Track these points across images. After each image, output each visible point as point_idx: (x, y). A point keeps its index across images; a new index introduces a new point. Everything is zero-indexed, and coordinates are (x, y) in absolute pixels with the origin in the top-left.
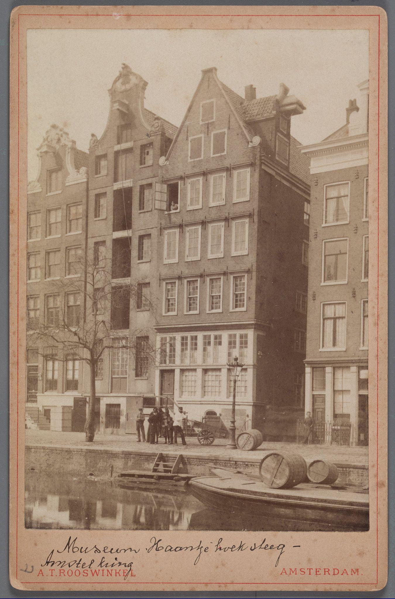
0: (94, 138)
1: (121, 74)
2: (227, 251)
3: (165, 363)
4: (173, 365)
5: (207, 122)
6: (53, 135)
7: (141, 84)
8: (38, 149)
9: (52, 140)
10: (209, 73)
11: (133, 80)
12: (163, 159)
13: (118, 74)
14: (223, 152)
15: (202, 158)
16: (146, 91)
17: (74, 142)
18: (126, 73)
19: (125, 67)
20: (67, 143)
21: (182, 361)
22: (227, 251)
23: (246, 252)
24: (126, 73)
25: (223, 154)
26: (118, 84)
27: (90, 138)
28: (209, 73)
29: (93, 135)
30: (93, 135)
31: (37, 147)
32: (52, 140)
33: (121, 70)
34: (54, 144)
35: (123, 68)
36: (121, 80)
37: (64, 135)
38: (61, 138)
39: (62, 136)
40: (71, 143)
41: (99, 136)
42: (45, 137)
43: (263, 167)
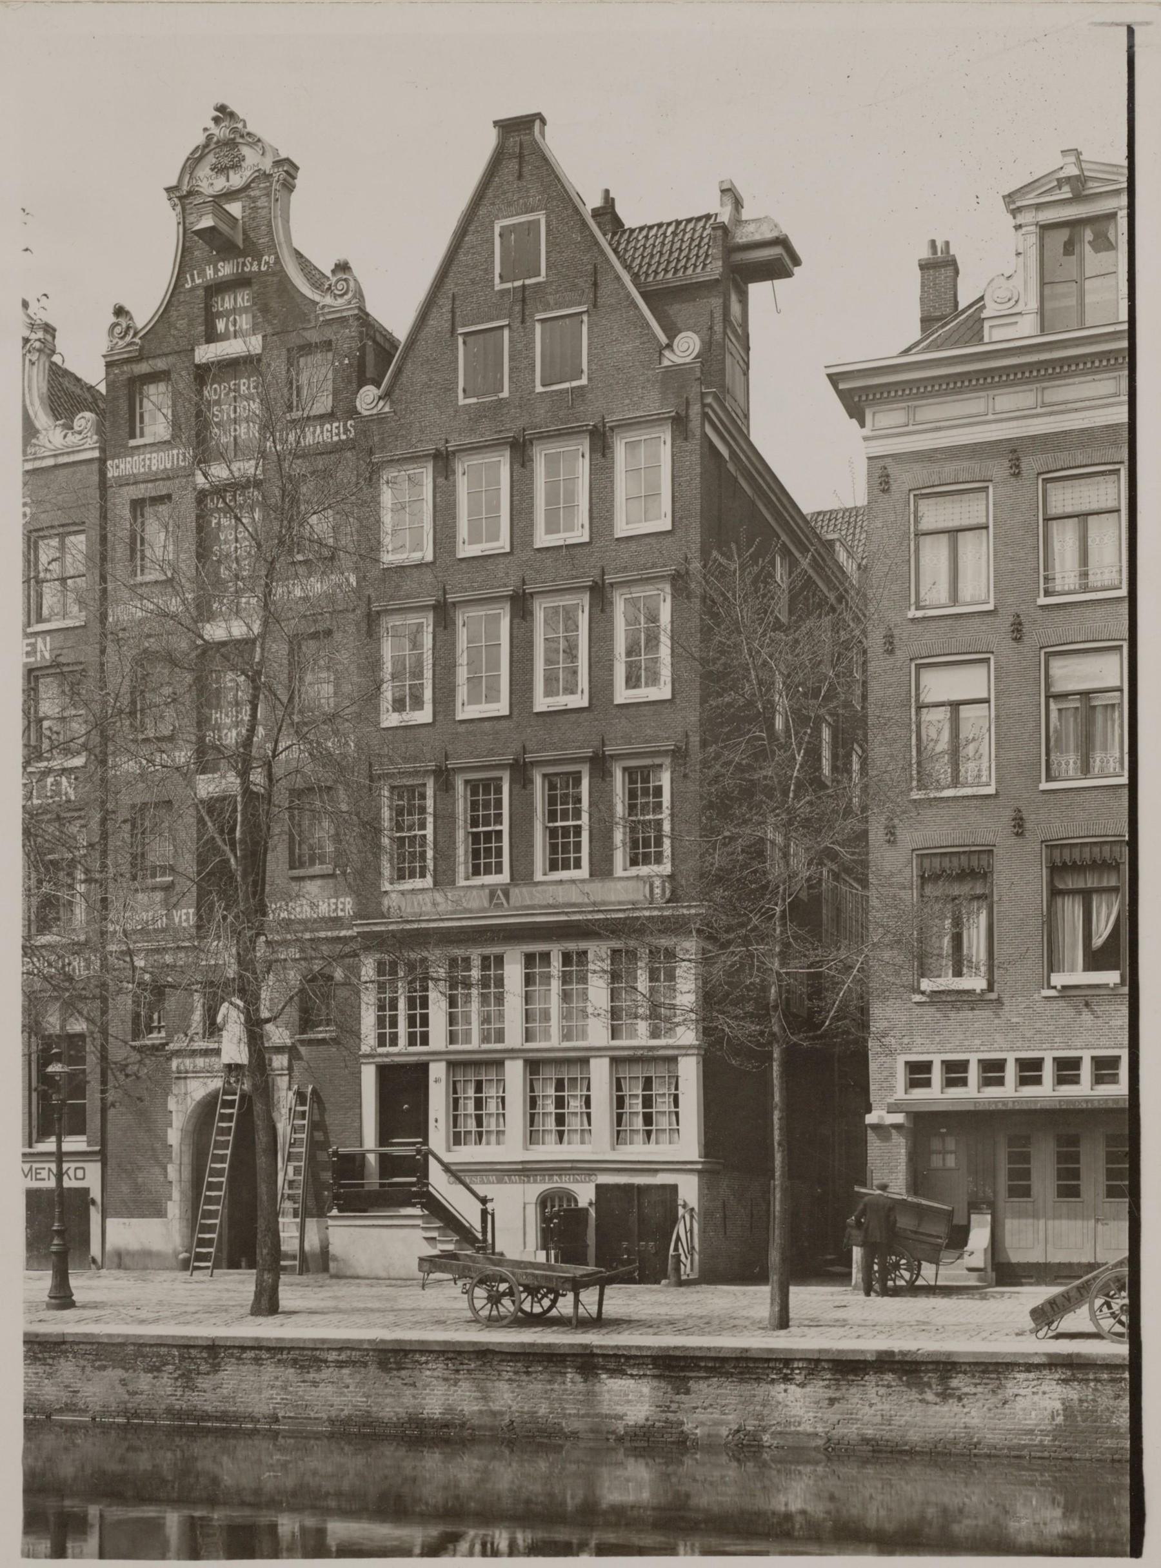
1: (209, 138)
2: (601, 686)
5: (518, 283)
7: (279, 174)
10: (519, 138)
12: (369, 393)
13: (200, 139)
14: (578, 375)
15: (505, 394)
16: (294, 196)
18: (227, 139)
19: (223, 113)
22: (601, 686)
23: (663, 691)
24: (227, 139)
25: (575, 384)
27: (113, 319)
29: (120, 311)
30: (120, 311)
33: (211, 124)
35: (216, 120)
36: (211, 159)
41: (143, 315)
43: (709, 430)
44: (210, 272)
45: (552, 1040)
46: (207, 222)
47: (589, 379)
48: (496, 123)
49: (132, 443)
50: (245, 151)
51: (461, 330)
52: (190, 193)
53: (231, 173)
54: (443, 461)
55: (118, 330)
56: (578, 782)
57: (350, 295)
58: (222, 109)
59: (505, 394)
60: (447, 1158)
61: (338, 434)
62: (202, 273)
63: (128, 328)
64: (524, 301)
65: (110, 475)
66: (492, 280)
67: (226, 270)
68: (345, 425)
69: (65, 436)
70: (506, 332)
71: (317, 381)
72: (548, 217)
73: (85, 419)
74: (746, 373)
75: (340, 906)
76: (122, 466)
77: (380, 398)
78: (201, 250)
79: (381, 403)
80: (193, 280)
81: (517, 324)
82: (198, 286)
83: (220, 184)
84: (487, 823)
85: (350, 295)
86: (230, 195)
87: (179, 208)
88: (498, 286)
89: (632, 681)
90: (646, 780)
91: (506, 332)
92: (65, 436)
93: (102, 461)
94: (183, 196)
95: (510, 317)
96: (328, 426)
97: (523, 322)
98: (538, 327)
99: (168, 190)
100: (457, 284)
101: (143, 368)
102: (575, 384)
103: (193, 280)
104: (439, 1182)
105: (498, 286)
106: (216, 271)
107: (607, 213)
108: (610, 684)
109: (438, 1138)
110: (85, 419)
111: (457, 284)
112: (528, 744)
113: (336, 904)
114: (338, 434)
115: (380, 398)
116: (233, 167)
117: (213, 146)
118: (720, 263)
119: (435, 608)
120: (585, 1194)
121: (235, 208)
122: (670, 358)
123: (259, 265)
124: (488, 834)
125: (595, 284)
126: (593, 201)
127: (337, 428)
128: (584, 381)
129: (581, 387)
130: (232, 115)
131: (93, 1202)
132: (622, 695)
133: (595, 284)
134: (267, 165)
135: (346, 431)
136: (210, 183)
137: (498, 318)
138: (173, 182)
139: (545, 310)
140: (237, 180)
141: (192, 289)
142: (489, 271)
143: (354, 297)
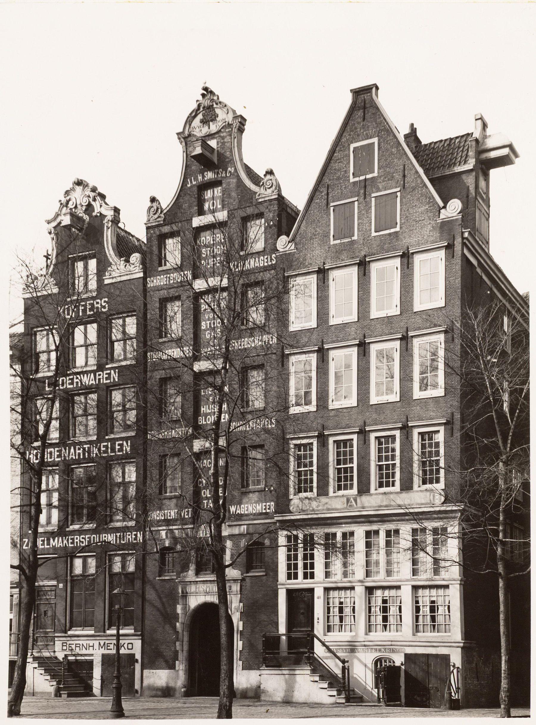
0: (155, 205)
1: (199, 106)
3: (296, 577)
4: (312, 580)
5: (362, 178)
6: (79, 197)
7: (236, 124)
8: (49, 222)
9: (76, 207)
11: (222, 115)
12: (283, 239)
13: (195, 106)
15: (355, 238)
17: (117, 210)
19: (207, 92)
20: (104, 212)
21: (327, 575)
25: (392, 230)
26: (197, 122)
27: (149, 204)
28: (364, 102)
31: (51, 216)
32: (76, 207)
33: (200, 98)
34: (80, 212)
35: (203, 95)
36: (200, 117)
37: (98, 198)
38: (93, 203)
39: (94, 200)
40: (112, 213)
41: (166, 200)
42: (64, 200)
43: (466, 251)
44: (200, 178)
45: (380, 578)
46: (198, 150)
47: (401, 228)
48: (351, 91)
49: (160, 269)
50: (218, 111)
51: (332, 204)
52: (190, 135)
53: (211, 123)
54: (322, 273)
55: (152, 210)
56: (394, 441)
57: (274, 187)
58: (206, 89)
59: (355, 238)
60: (322, 638)
61: (267, 262)
62: (196, 179)
63: (158, 209)
64: (365, 187)
65: (149, 286)
66: (349, 177)
67: (210, 175)
68: (271, 257)
69: (126, 266)
70: (356, 203)
71: (257, 232)
72: (379, 140)
73: (135, 257)
74: (488, 219)
75: (268, 507)
76: (155, 281)
77: (289, 242)
78: (195, 166)
79: (290, 244)
80: (191, 182)
81: (362, 199)
82: (194, 185)
83: (205, 130)
84: (345, 463)
85: (274, 187)
86: (211, 136)
87: (184, 144)
88: (352, 180)
89: (424, 386)
90: (431, 439)
91: (356, 203)
92: (126, 266)
93: (145, 278)
94: (186, 138)
95: (358, 196)
96: (262, 258)
97: (365, 198)
98: (373, 199)
99: (178, 134)
100: (330, 180)
101: (166, 229)
102: (392, 230)
103: (191, 182)
104: (319, 650)
105: (352, 180)
106: (203, 177)
107: (412, 136)
108: (411, 389)
109: (319, 629)
110: (135, 257)
111: (330, 180)
112: (367, 421)
113: (265, 506)
114: (267, 262)
115: (289, 242)
116: (212, 121)
117: (201, 109)
118: (474, 160)
119: (317, 351)
120: (398, 660)
121: (213, 143)
122: (444, 214)
123: (226, 173)
124: (346, 469)
125: (404, 176)
126: (403, 130)
127: (267, 258)
128: (398, 229)
129: (396, 233)
130: (212, 92)
131: (137, 661)
132: (417, 394)
133: (404, 176)
134: (230, 118)
135: (271, 259)
136: (199, 130)
137: (352, 197)
138: (181, 130)
139: (377, 192)
140: (214, 128)
141: (191, 187)
142: (347, 172)
143: (276, 189)
